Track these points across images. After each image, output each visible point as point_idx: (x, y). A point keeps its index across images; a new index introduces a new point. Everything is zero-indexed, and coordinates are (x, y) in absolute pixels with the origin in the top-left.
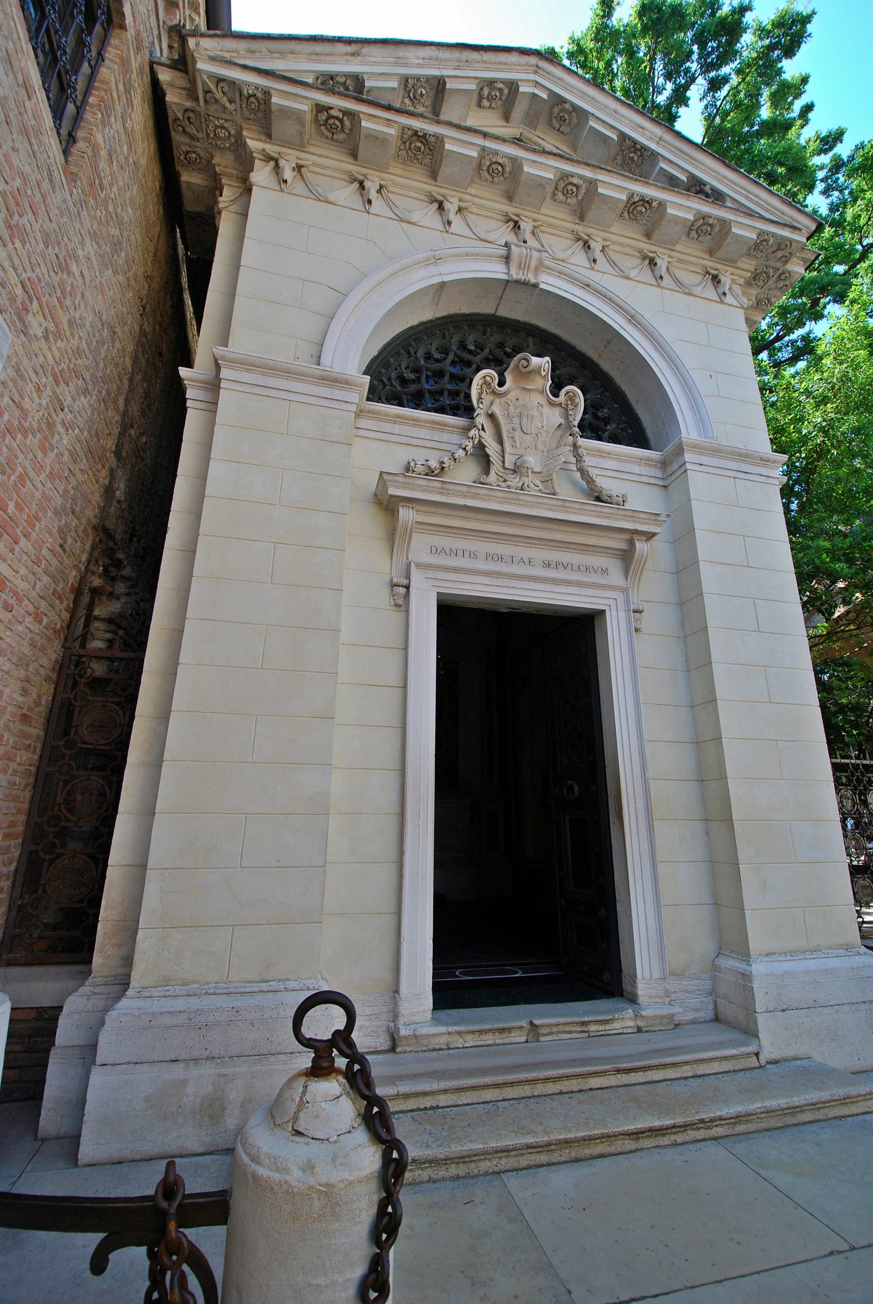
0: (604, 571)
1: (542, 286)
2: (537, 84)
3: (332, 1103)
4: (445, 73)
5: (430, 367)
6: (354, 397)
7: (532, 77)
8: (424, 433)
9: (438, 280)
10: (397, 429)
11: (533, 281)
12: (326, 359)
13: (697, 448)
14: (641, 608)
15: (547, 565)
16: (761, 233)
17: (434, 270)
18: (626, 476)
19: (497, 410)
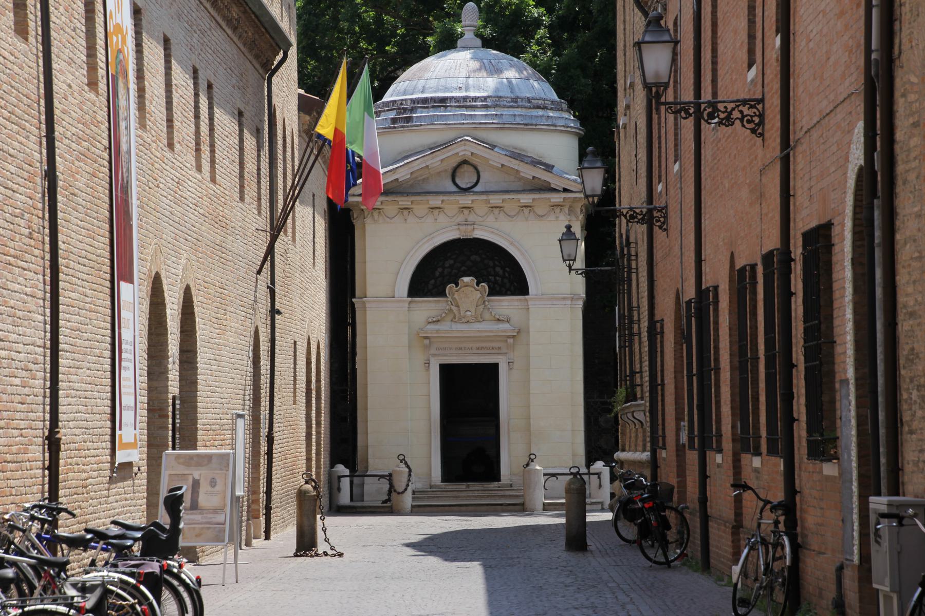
0: (499, 348)
3: (403, 465)
4: (428, 163)
6: (407, 305)
7: (463, 148)
8: (433, 305)
12: (396, 295)
13: (531, 299)
15: (478, 349)
16: (564, 199)
19: (456, 296)
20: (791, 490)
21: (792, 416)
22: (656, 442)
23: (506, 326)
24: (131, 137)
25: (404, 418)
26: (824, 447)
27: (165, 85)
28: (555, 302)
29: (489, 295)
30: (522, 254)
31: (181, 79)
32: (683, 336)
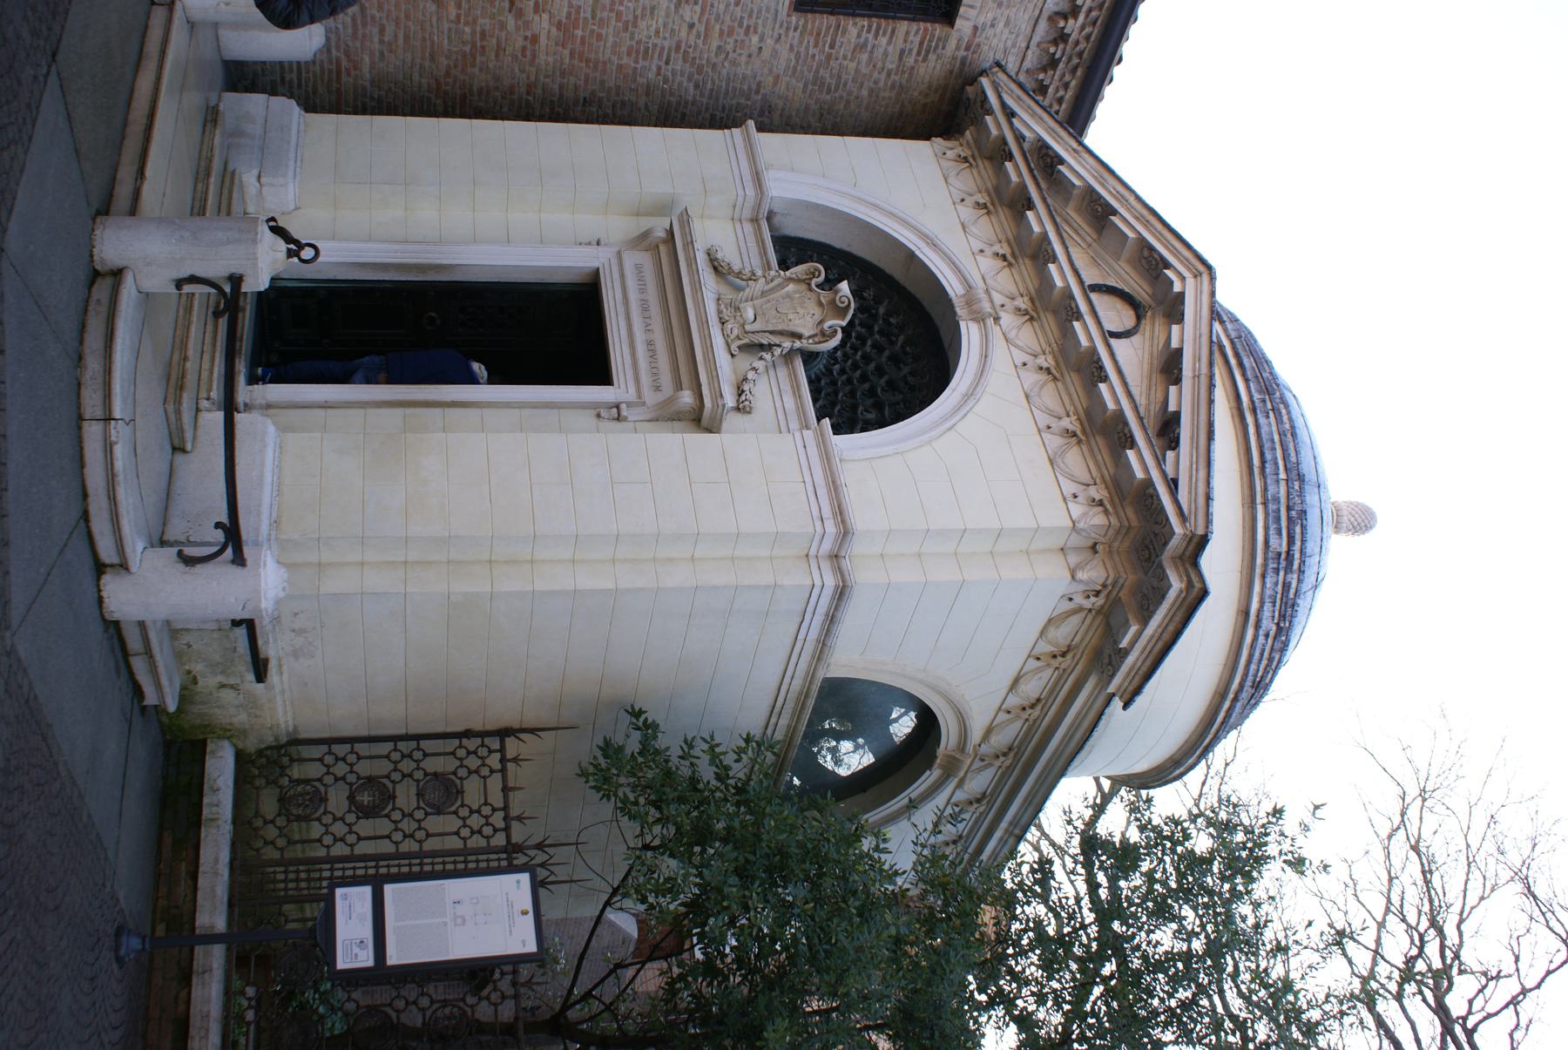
0: (658, 389)
1: (963, 325)
2: (1183, 279)
4: (1122, 211)
9: (913, 248)
10: (752, 245)
11: (960, 311)
14: (624, 413)
15: (650, 343)
17: (921, 244)
18: (781, 417)
23: (730, 401)
28: (822, 492)
29: (809, 357)
30: (945, 419)
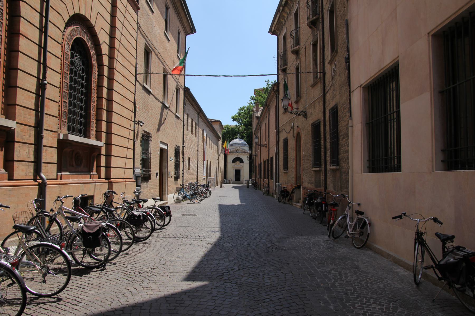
5: (234, 161)
20: (269, 182)
21: (269, 175)
22: (256, 178)
24: (206, 147)
25: (231, 175)
26: (272, 178)
27: (209, 142)
31: (210, 141)
32: (259, 167)
